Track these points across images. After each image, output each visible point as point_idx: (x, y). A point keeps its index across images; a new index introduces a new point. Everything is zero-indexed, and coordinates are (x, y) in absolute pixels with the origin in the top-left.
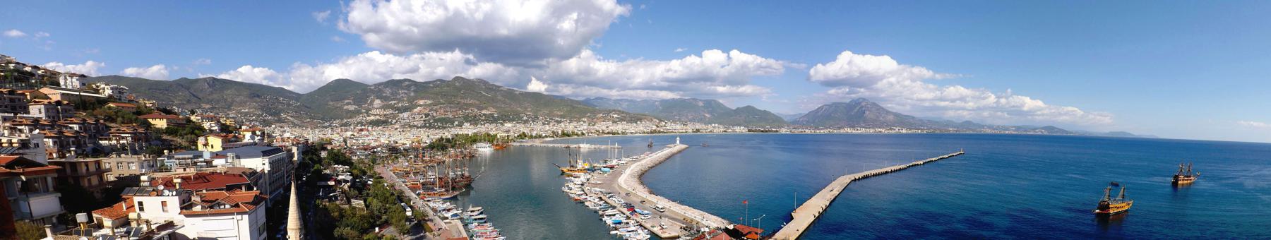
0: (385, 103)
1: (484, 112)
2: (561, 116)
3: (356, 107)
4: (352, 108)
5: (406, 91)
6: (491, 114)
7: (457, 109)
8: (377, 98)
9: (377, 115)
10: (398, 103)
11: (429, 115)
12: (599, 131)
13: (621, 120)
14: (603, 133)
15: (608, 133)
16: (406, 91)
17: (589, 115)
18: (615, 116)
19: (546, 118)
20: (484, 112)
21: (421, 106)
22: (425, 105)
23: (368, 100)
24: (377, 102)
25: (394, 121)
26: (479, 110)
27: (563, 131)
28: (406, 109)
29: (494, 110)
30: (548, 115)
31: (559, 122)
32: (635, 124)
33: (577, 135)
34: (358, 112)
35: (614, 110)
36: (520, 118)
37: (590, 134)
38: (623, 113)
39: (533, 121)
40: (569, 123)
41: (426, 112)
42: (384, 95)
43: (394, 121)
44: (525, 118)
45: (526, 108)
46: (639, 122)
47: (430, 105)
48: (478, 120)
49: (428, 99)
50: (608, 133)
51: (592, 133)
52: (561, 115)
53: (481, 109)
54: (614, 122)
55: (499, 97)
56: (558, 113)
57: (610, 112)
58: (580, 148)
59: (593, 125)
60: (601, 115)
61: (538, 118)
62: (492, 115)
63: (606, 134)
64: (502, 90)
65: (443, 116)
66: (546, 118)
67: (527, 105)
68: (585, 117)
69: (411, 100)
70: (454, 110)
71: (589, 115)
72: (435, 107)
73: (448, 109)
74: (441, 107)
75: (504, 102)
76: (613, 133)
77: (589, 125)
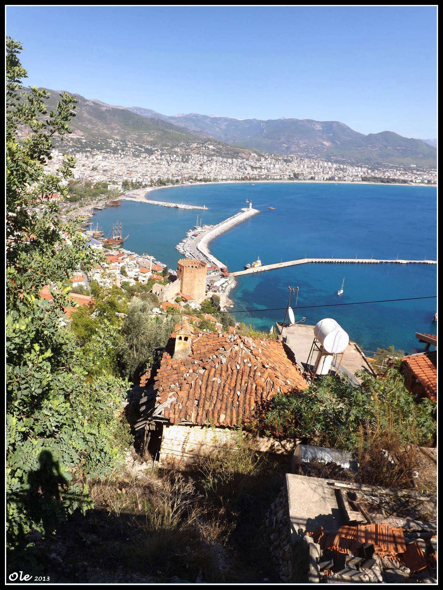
6: (78, 139)
15: (201, 180)
18: (211, 147)
19: (135, 145)
29: (82, 134)
35: (209, 140)
36: (108, 145)
44: (113, 145)
45: (113, 129)
48: (65, 146)
50: (201, 180)
52: (151, 142)
56: (149, 139)
62: (79, 140)
64: (88, 105)
67: (113, 125)
75: (90, 122)
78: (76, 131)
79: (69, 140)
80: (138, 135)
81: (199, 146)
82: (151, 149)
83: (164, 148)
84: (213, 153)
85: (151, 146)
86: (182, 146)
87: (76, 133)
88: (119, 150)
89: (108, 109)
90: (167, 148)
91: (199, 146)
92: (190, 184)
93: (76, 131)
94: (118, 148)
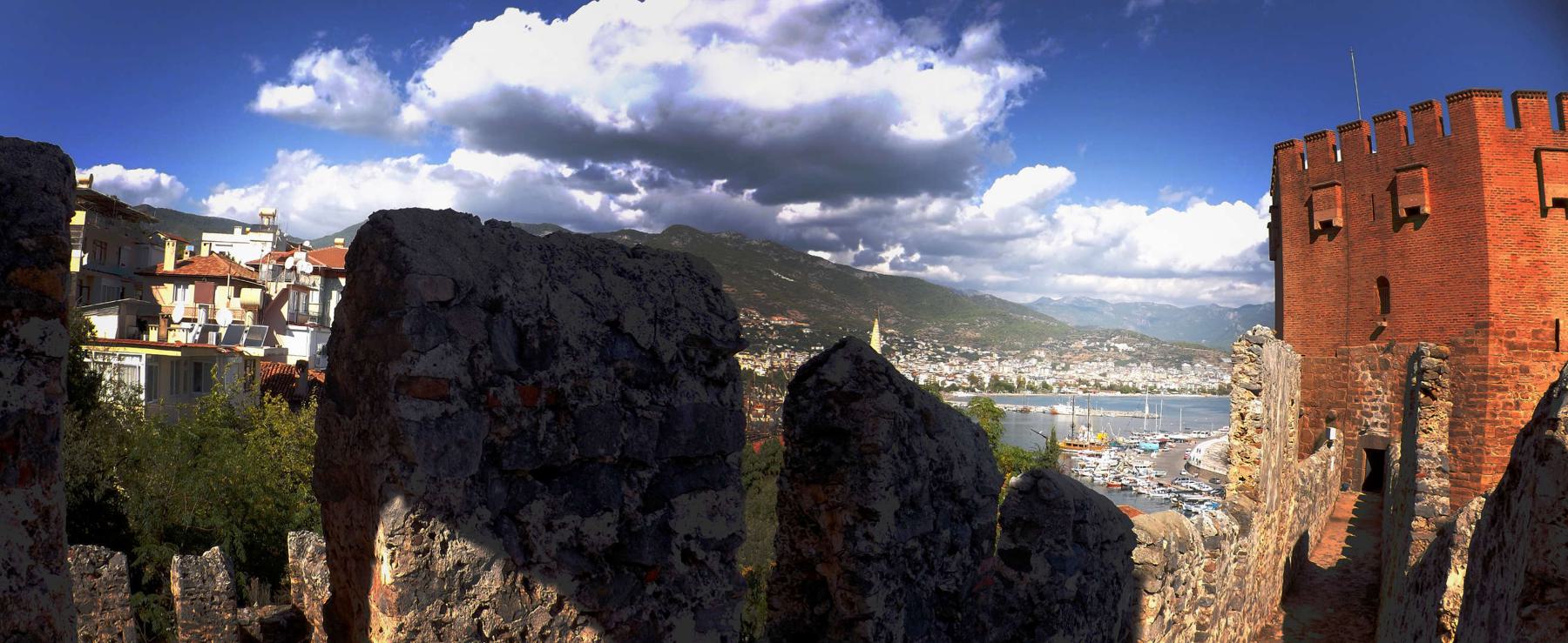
1: (776, 320)
2: (976, 343)
12: (1086, 383)
13: (1139, 358)
14: (1098, 385)
15: (1111, 388)
17: (1050, 341)
18: (1122, 347)
20: (776, 320)
26: (762, 314)
27: (995, 378)
30: (940, 337)
31: (973, 358)
32: (1175, 371)
33: (1031, 388)
35: (1118, 332)
37: (1065, 389)
38: (1142, 339)
39: (905, 353)
40: (1000, 360)
46: (1185, 365)
50: (1111, 388)
51: (1068, 386)
52: (976, 340)
53: (768, 312)
54: (1119, 363)
55: (813, 286)
56: (969, 334)
57: (1107, 335)
58: (1055, 413)
59: (1066, 369)
60: (1084, 343)
61: (915, 345)
62: (796, 330)
63: (1104, 389)
64: (822, 268)
66: (935, 346)
68: (1040, 346)
71: (1050, 341)
76: (1124, 390)
77: (1054, 367)
78: (789, 312)
79: (771, 328)
80: (943, 327)
81: (1092, 344)
82: (976, 353)
83: (1006, 353)
84: (1128, 358)
85: (974, 347)
86: (1051, 346)
87: (788, 316)
88: (894, 351)
89: (871, 275)
90: (1013, 353)
91: (1092, 344)
92: (1080, 393)
93: (789, 312)
94: (894, 348)
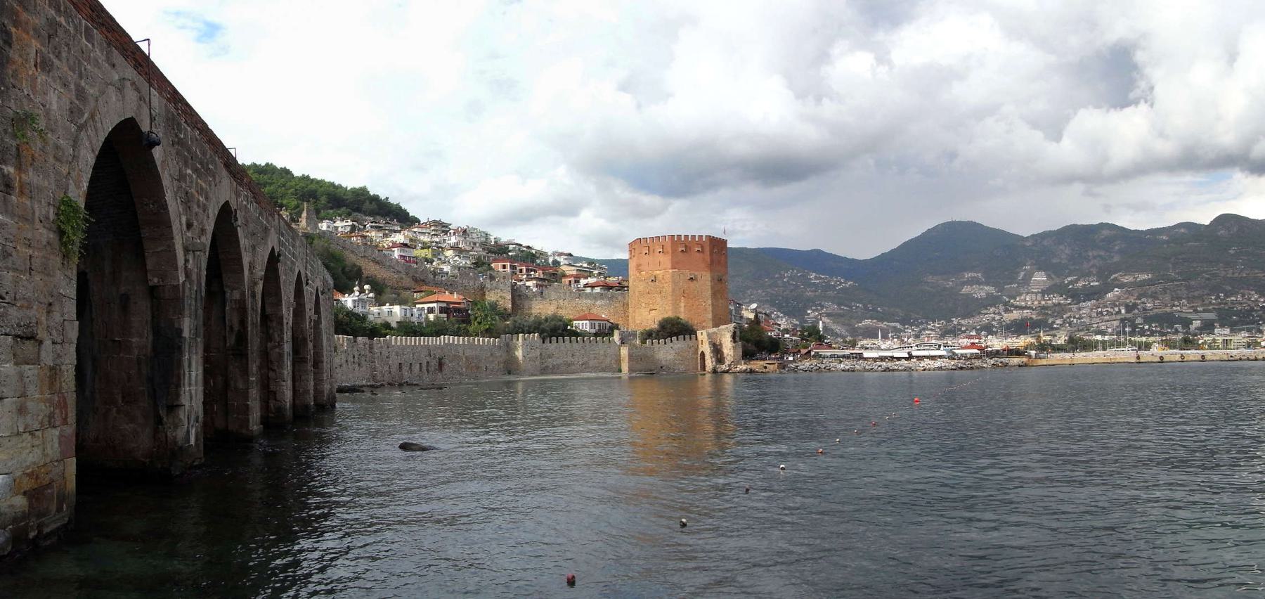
0: (1057, 281)
3: (990, 289)
4: (980, 292)
5: (1102, 253)
7: (1206, 291)
8: (1039, 269)
9: (1026, 308)
10: (1077, 281)
11: (1135, 306)
16: (1102, 253)
21: (1121, 286)
22: (1134, 285)
23: (1018, 273)
24: (1040, 278)
25: (1059, 321)
28: (1090, 294)
34: (991, 301)
41: (1131, 300)
42: (1055, 261)
43: (1059, 321)
47: (1142, 284)
49: (1142, 271)
65: (1168, 310)
69: (1103, 274)
70: (1196, 294)
72: (1153, 288)
73: (1184, 292)
74: (1165, 290)
